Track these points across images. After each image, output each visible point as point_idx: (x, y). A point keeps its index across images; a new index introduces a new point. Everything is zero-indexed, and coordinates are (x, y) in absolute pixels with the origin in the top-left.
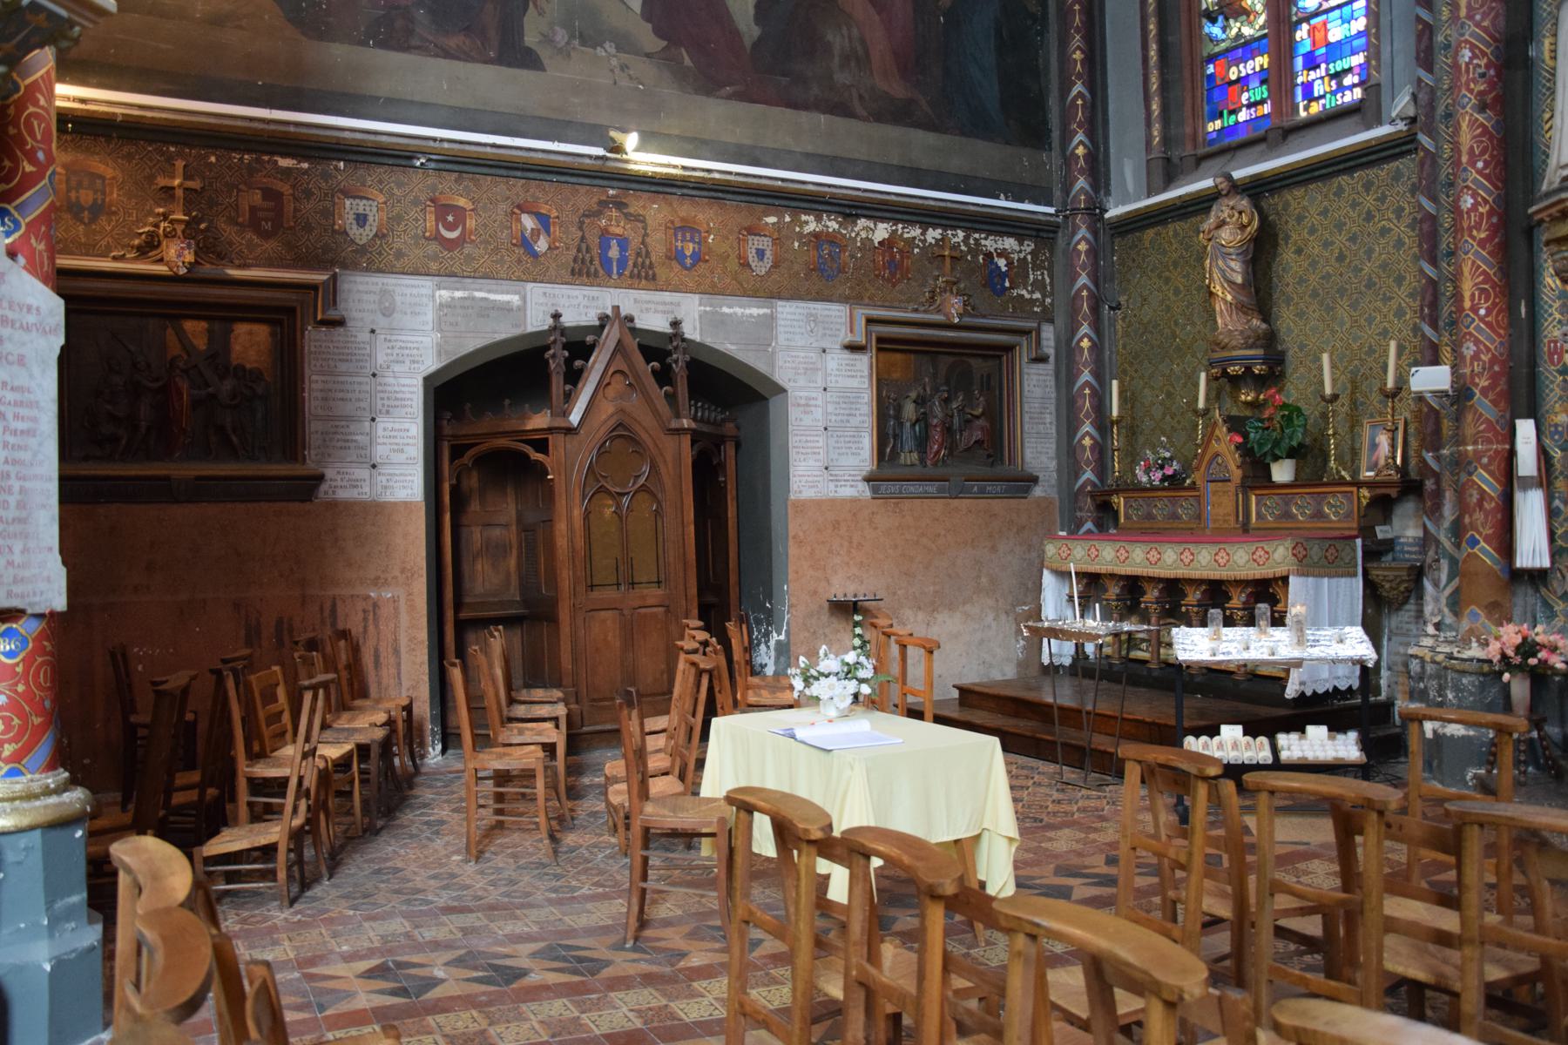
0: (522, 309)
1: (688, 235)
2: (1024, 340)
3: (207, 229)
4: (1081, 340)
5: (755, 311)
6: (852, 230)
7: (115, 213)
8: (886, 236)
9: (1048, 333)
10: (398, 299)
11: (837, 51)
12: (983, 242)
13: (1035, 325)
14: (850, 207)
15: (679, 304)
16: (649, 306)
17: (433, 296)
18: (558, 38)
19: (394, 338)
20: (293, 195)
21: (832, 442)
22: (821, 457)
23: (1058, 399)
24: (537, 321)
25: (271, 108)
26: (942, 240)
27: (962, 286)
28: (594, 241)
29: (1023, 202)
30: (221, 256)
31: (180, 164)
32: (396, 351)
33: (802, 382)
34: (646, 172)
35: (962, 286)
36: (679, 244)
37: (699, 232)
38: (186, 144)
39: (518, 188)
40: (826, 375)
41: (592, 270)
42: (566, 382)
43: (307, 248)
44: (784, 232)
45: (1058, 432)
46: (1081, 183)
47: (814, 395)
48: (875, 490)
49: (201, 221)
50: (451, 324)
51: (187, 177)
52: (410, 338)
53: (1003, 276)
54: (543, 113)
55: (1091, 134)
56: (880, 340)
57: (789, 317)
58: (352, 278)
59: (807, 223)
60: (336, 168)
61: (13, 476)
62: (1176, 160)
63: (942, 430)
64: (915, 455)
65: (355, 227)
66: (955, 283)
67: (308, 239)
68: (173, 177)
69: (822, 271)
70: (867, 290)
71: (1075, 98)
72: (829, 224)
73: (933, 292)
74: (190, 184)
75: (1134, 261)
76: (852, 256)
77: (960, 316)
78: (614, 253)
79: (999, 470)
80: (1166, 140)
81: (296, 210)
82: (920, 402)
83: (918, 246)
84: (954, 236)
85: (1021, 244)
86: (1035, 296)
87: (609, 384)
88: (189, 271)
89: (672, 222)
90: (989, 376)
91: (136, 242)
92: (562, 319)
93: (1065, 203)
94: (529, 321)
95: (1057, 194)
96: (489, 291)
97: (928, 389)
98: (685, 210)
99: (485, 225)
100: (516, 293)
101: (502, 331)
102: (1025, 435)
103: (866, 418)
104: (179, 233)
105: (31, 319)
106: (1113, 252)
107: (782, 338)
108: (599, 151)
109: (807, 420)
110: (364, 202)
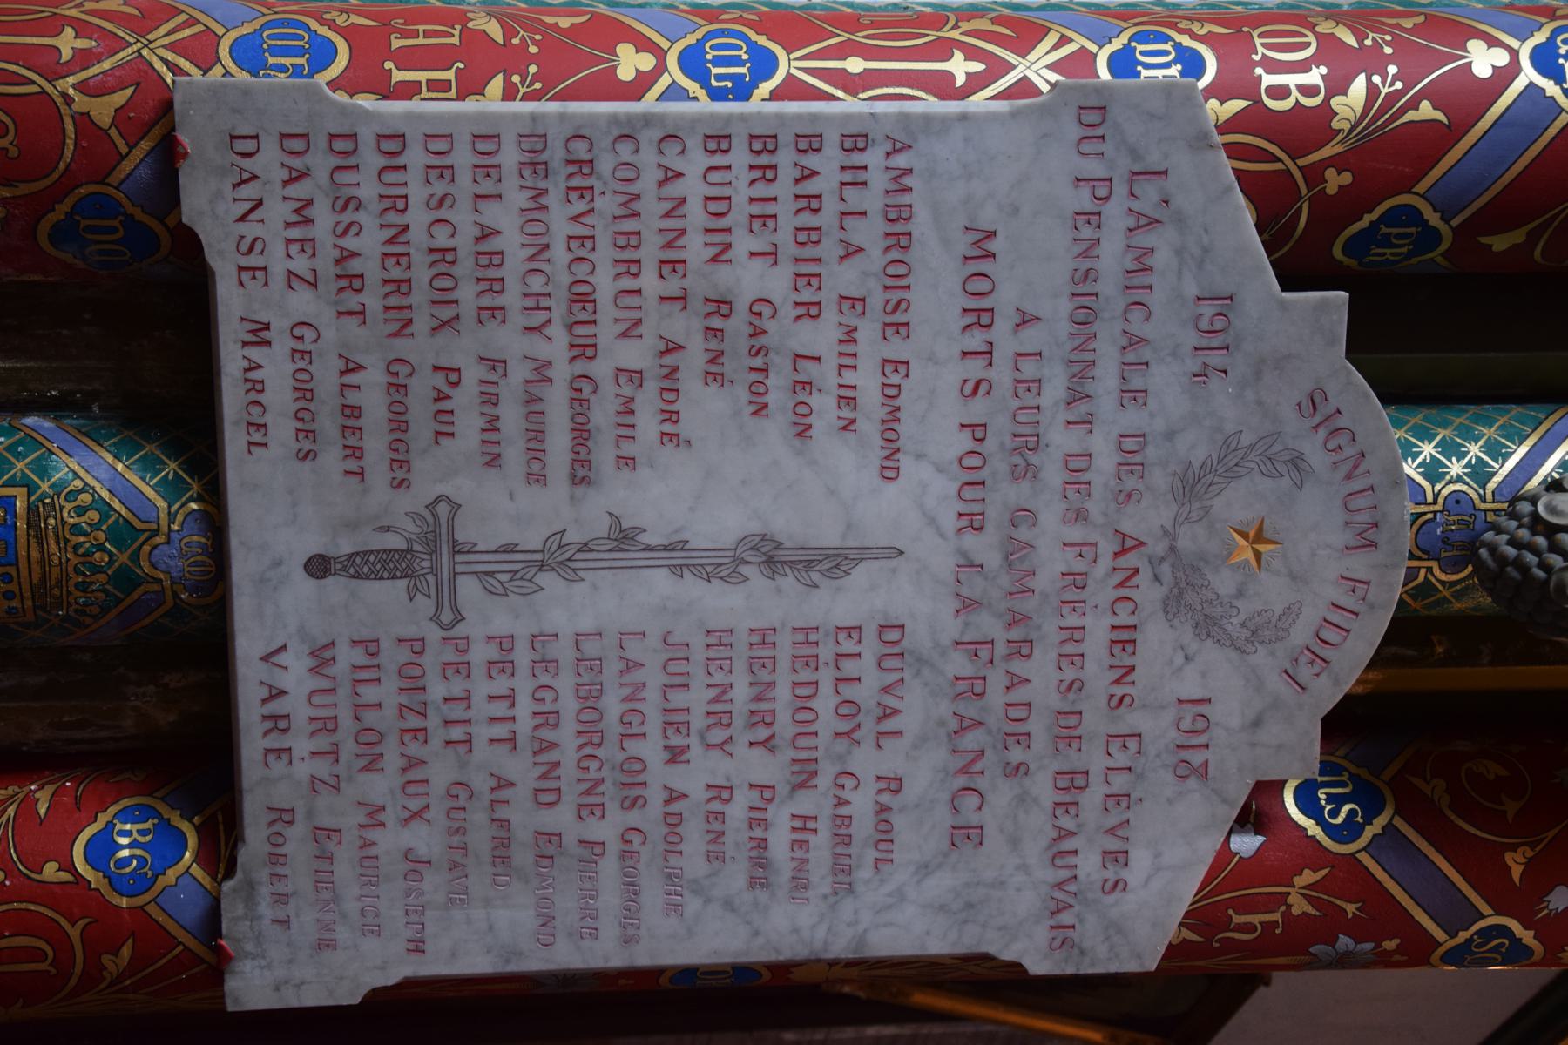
61: (633, 818)
105: (1089, 865)
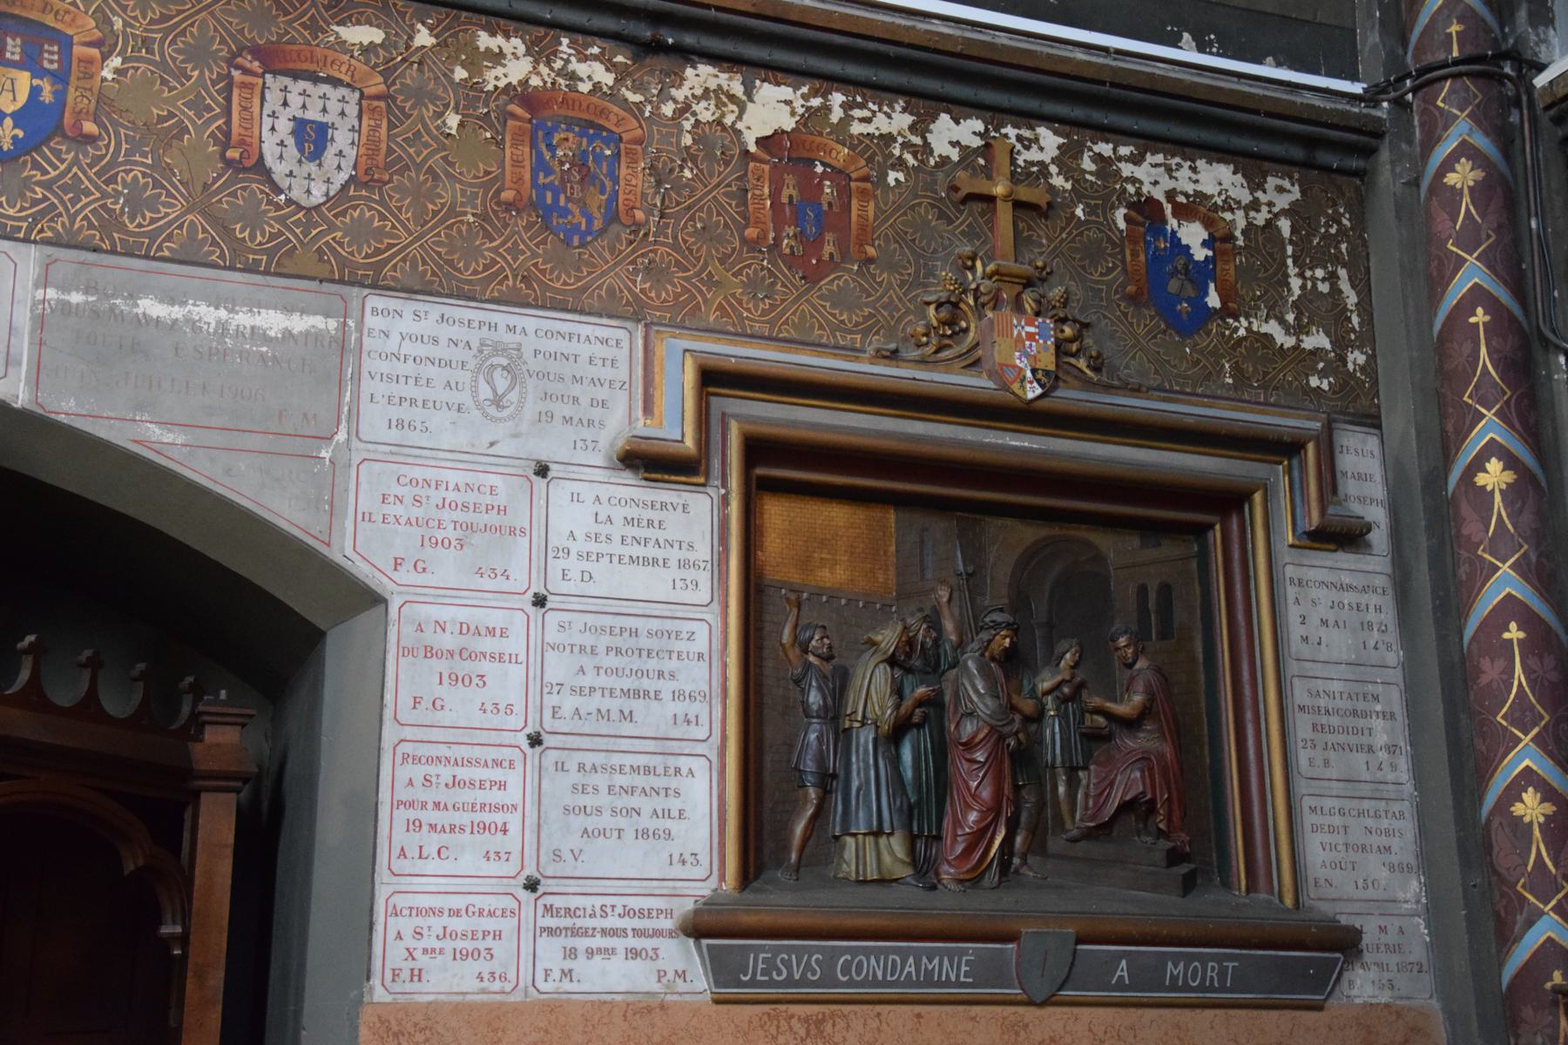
2: (1279, 476)
4: (1478, 465)
5: (273, 321)
6: (663, 96)
8: (789, 124)
12: (1127, 169)
21: (559, 788)
22: (512, 842)
27: (1056, 293)
35: (1056, 293)
37: (66, 43)
47: (495, 618)
48: (722, 970)
53: (1200, 274)
56: (758, 449)
57: (408, 348)
59: (498, 57)
63: (994, 757)
64: (896, 846)
72: (582, 69)
73: (952, 307)
79: (1209, 904)
83: (900, 164)
84: (1027, 144)
85: (1256, 184)
86: (1309, 343)
90: (1165, 590)
93: (1393, 59)
95: (1370, 39)
97: (949, 626)
102: (1301, 787)
103: (698, 708)
107: (374, 421)
109: (462, 706)
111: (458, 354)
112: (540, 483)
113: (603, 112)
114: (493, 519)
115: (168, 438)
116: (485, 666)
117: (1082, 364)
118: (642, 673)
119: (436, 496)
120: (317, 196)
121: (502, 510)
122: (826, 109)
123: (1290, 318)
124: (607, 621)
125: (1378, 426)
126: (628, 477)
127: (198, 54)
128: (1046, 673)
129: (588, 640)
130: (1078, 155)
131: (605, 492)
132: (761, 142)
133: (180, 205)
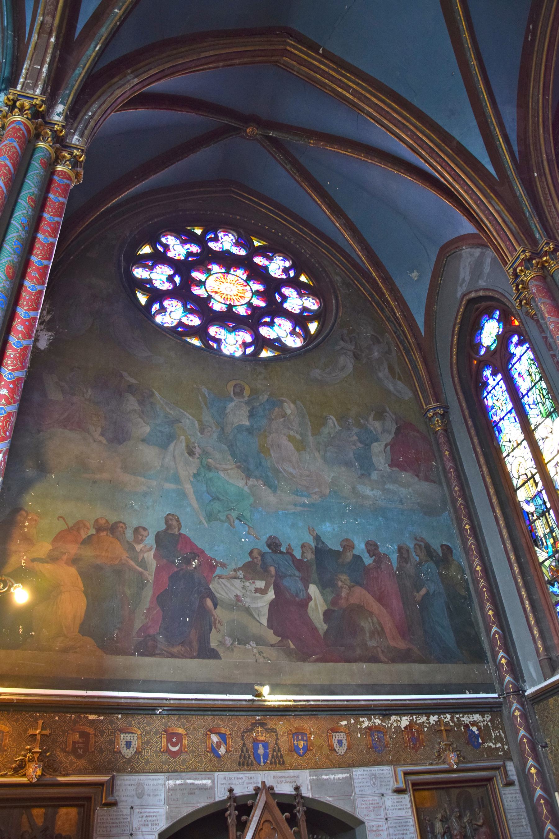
0: (213, 788)
1: (300, 737)
2: (497, 773)
3: (50, 756)
5: (340, 776)
6: (389, 723)
7: (6, 751)
8: (408, 723)
9: (511, 767)
10: (146, 787)
11: (367, 630)
12: (462, 719)
13: (502, 763)
14: (386, 710)
15: (298, 777)
16: (281, 779)
17: (165, 785)
18: (227, 642)
19: (143, 810)
20: (95, 734)
23: (527, 807)
24: (221, 795)
25: (87, 690)
26: (439, 721)
27: (455, 746)
28: (250, 745)
29: (479, 693)
30: (55, 770)
31: (41, 722)
32: (144, 819)
33: (372, 816)
34: (275, 706)
35: (455, 746)
36: (296, 742)
37: (306, 734)
38: (44, 712)
39: (208, 721)
40: (386, 810)
41: (250, 762)
42: (237, 830)
43: (100, 762)
44: (352, 729)
45: (532, 830)
46: (508, 678)
47: (380, 823)
49: (48, 751)
50: (174, 800)
51: (43, 728)
52: (152, 810)
53: (477, 737)
54: (222, 681)
55: (507, 651)
56: (414, 784)
57: (361, 777)
58: (122, 778)
59: (363, 722)
60: (117, 718)
62: (554, 658)
65: (125, 748)
66: (450, 745)
67: (101, 757)
68: (37, 730)
69: (376, 748)
70: (402, 756)
71: (494, 634)
72: (376, 721)
74: (45, 732)
75: (547, 717)
76: (391, 737)
77: (457, 764)
78: (261, 751)
80: (546, 649)
81: (95, 742)
82: (444, 820)
83: (426, 727)
85: (483, 717)
87: (262, 829)
88: (38, 780)
89: (291, 730)
90: (482, 798)
91: (14, 765)
92: (235, 792)
93: (502, 690)
94: (216, 795)
95: (497, 686)
96: (194, 779)
97: (448, 811)
98: (297, 723)
99: (192, 742)
100: (209, 779)
101: (202, 802)
104: (36, 759)
106: (535, 713)
107: (357, 790)
108: (250, 697)
110: (130, 735)
111: (367, 776)
112: (383, 797)
113: (380, 728)
114: (376, 805)
115: (330, 799)
116: (381, 832)
117: (461, 758)
118: (403, 830)
119: (368, 802)
120: (343, 753)
121: (378, 803)
122: (413, 719)
123: (494, 741)
124: (397, 821)
125: (512, 760)
126: (395, 794)
127: (323, 732)
128: (465, 818)
129: (395, 825)
130: (454, 718)
131: (392, 797)
132: (404, 728)
133: (325, 758)
